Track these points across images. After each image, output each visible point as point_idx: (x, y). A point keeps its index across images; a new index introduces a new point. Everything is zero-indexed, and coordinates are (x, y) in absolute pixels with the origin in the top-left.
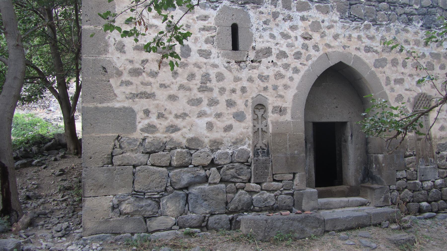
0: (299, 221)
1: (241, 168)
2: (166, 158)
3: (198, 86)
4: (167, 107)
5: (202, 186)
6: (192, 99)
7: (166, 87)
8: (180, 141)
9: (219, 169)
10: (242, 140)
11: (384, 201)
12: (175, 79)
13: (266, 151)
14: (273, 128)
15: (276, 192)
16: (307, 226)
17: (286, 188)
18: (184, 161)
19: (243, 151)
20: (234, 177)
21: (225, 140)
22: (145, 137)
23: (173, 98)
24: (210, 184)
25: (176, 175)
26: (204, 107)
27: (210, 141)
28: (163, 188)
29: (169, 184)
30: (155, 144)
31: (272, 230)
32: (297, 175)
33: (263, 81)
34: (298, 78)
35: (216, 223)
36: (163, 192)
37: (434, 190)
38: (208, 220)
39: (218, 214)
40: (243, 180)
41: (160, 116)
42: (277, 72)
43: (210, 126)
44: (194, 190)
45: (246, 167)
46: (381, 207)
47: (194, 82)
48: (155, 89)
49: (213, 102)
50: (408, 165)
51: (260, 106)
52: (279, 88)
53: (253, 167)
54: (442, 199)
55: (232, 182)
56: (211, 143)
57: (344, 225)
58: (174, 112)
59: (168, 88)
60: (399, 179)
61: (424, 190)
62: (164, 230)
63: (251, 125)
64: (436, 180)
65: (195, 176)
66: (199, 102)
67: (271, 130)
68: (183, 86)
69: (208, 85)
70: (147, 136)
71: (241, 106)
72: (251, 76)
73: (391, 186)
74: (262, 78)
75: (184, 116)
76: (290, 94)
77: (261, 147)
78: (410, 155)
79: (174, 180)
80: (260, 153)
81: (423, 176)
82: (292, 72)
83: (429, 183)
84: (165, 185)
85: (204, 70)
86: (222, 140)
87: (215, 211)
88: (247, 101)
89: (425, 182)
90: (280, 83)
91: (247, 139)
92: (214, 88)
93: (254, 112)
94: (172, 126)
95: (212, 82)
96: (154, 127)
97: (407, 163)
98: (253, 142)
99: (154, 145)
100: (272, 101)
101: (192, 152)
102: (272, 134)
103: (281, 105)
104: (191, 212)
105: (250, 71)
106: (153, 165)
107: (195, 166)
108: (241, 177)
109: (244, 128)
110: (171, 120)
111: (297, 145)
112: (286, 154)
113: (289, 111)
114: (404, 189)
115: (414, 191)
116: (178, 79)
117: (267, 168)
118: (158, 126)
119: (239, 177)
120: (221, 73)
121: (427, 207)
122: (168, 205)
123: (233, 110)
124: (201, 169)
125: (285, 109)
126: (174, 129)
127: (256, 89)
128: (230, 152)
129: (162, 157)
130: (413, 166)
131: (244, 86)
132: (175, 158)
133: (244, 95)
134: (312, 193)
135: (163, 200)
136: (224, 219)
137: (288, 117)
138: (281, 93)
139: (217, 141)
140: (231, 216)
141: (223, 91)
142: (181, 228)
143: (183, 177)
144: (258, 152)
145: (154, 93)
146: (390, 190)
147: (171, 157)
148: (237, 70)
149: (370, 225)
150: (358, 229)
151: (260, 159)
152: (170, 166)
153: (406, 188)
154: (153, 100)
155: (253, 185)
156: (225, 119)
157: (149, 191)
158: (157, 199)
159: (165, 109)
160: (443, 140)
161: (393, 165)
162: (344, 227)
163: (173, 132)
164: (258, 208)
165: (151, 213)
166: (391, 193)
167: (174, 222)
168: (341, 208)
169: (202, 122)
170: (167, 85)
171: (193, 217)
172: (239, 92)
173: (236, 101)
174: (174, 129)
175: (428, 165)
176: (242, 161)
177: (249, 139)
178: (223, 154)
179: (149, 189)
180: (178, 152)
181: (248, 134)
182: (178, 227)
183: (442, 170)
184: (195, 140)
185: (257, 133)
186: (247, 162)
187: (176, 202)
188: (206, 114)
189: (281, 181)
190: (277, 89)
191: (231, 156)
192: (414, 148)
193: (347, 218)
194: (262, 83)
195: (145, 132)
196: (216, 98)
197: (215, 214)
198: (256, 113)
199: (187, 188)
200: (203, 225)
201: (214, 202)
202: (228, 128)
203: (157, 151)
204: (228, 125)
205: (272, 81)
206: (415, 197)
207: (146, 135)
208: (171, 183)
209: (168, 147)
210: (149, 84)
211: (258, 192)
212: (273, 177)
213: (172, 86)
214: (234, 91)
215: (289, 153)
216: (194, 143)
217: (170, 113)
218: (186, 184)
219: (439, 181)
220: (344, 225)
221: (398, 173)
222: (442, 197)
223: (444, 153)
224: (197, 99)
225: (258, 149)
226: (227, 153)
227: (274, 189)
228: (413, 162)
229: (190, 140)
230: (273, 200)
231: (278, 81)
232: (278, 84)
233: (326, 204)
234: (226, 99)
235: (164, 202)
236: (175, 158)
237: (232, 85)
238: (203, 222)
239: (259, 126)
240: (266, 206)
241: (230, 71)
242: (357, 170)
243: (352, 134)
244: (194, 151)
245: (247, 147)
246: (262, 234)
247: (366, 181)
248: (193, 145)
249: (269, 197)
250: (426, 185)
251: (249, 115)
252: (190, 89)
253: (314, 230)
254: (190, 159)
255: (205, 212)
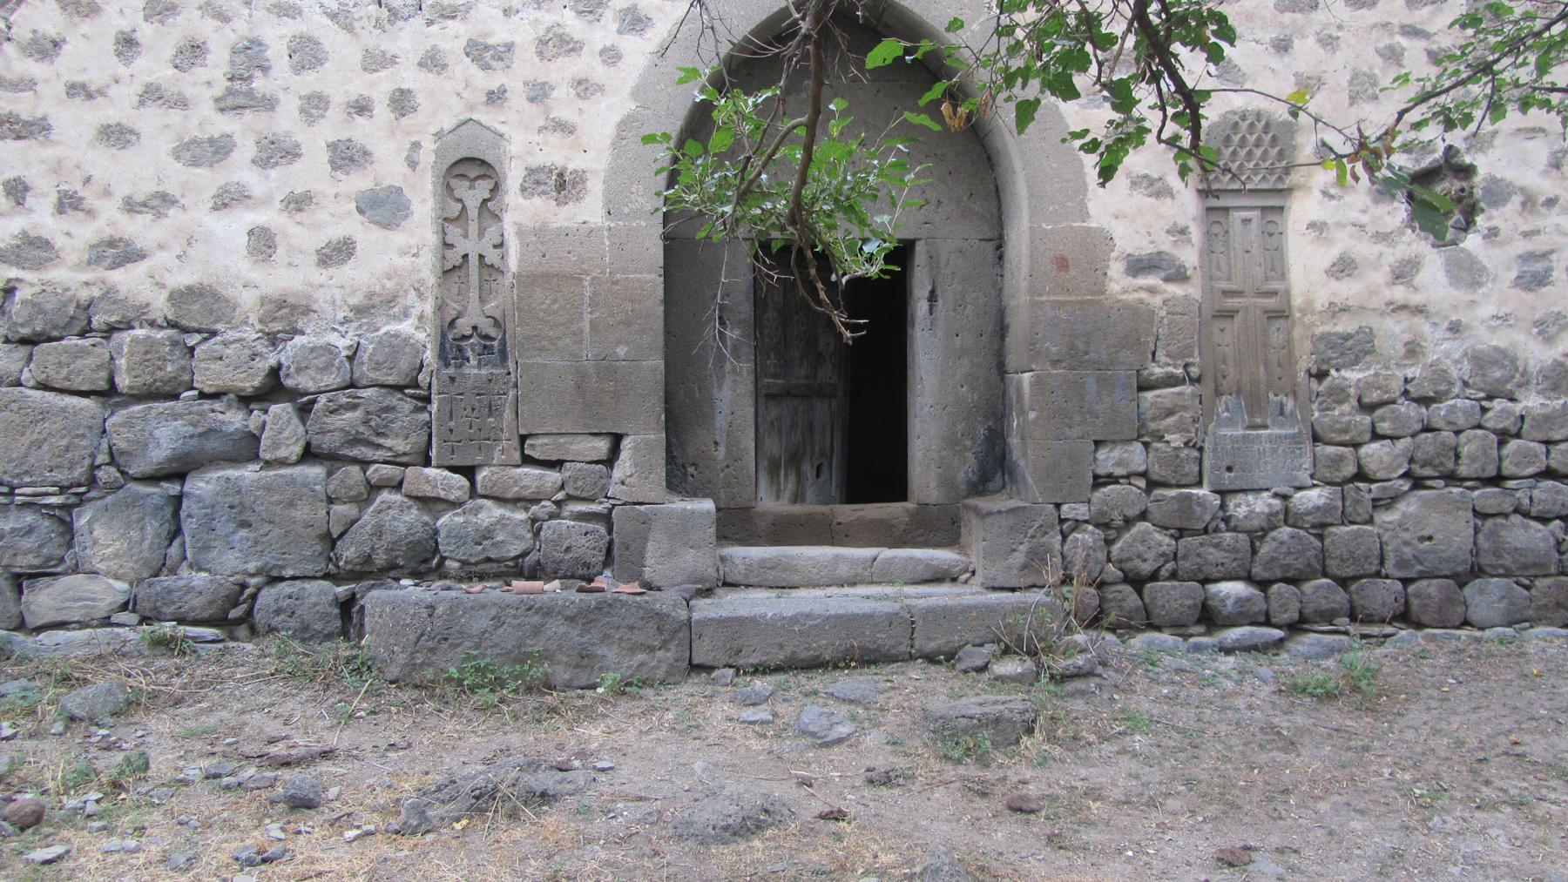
0: (571, 619)
1: (388, 409)
2: (90, 361)
3: (219, 90)
4: (93, 172)
5: (233, 473)
6: (194, 141)
7: (90, 96)
8: (143, 300)
9: (304, 411)
10: (391, 300)
11: (1024, 567)
12: (128, 62)
13: (496, 343)
14: (523, 255)
15: (534, 508)
16: (605, 638)
17: (578, 493)
18: (159, 374)
19: (396, 342)
20: (357, 441)
21: (321, 299)
22: (9, 280)
23: (116, 135)
24: (268, 464)
25: (129, 424)
26: (240, 170)
27: (263, 301)
28: (79, 472)
29: (102, 458)
30: (49, 307)
31: (445, 645)
32: (626, 443)
33: (486, 67)
34: (638, 50)
35: (278, 612)
36: (80, 485)
37: (1285, 532)
38: (254, 597)
39: (293, 578)
40: (398, 455)
41: (68, 203)
42: (549, 30)
43: (263, 243)
44: (202, 485)
45: (407, 406)
46: (1013, 590)
47: (200, 73)
48: (47, 102)
49: (276, 152)
50: (1153, 419)
51: (470, 169)
52: (555, 94)
53: (434, 407)
54: (1325, 575)
55: (355, 461)
56: (267, 307)
57: (781, 646)
58: (122, 190)
59: (100, 99)
60: (1112, 479)
61: (1235, 529)
62: (83, 625)
63: (431, 238)
64: (1300, 488)
65: (200, 430)
66: (220, 149)
67: (513, 264)
68: (158, 89)
69: (259, 84)
70: (18, 280)
71: (389, 167)
72: (434, 47)
73: (1065, 508)
74: (481, 53)
75: (160, 203)
76: (601, 121)
77: (475, 328)
78: (1170, 381)
79: (122, 445)
80: (469, 354)
81: (1229, 469)
82: (615, 26)
84: (87, 462)
85: (240, 28)
86: (309, 297)
87: (283, 567)
88: (416, 145)
89: (1240, 498)
90: (562, 71)
91: (412, 293)
92: (281, 95)
93: (449, 188)
94: (112, 243)
95: (272, 72)
96: (43, 244)
97: (1149, 415)
98: (440, 308)
99: (42, 311)
100: (522, 146)
101: (192, 340)
102: (517, 276)
103: (560, 164)
104: (191, 566)
105: (435, 28)
106: (44, 386)
107: (203, 395)
108: (388, 442)
109: (402, 255)
110: (110, 219)
111: (628, 324)
112: (575, 356)
113: (596, 188)
114: (1129, 522)
115: (1181, 533)
116: (140, 63)
117: (492, 410)
118: (59, 241)
119: (381, 441)
120: (310, 39)
121: (1240, 601)
122: (95, 533)
123: (359, 182)
124: (229, 407)
125: (580, 178)
126: (121, 252)
127: (455, 100)
128: (343, 343)
129: (79, 358)
130: (1179, 428)
131: (405, 86)
132: (123, 361)
133: (405, 121)
134: (688, 516)
135: (79, 516)
136: (313, 599)
137: (589, 210)
138: (565, 113)
139: (291, 300)
140: (342, 590)
141: (317, 107)
142: (145, 620)
143: (157, 433)
144: (460, 349)
145: (44, 119)
146: (1062, 521)
147: (112, 358)
148: (378, 24)
149: (912, 658)
150: (848, 667)
151: (464, 376)
152: (108, 393)
153: (1143, 516)
154: (42, 144)
155: (436, 479)
156: (322, 216)
157: (27, 479)
158: (57, 512)
159: (88, 180)
160: (1345, 317)
161: (1077, 419)
162: (779, 657)
163: (115, 265)
164: (456, 565)
165: (36, 562)
166: (1064, 537)
167: (122, 599)
168: (840, 580)
169: (234, 227)
170: (93, 88)
171: (197, 583)
172: (382, 111)
173: (369, 148)
174: (121, 252)
175: (1265, 427)
176: (391, 380)
177: (420, 295)
178: (313, 350)
179: (26, 473)
180: (135, 340)
181: (415, 277)
182: (134, 618)
183: (1330, 449)
184: (201, 295)
185: (462, 273)
186: (417, 386)
187: (128, 526)
188: (248, 197)
189: (556, 464)
190: (546, 95)
191: (351, 359)
192: (1190, 347)
193: (794, 619)
194: (482, 73)
195: (11, 263)
196: (288, 134)
197: (282, 579)
198: (457, 194)
199: (179, 475)
200: (233, 615)
201: (277, 531)
202: (338, 253)
203: (55, 334)
204: (335, 239)
205: (526, 66)
206: (1185, 557)
207: (14, 273)
208: (111, 454)
209: (98, 321)
210: (29, 84)
211: (460, 504)
212: (522, 449)
213: (113, 91)
214: (362, 108)
215: (588, 352)
216: (196, 307)
217: (107, 193)
218: (170, 460)
219: (1313, 497)
220: (781, 646)
221: (1102, 454)
222: (1324, 566)
223: (1345, 373)
224: (211, 141)
225: (465, 338)
226: (329, 349)
227: (526, 493)
228: (1185, 408)
229: (181, 294)
230: (520, 538)
231: (552, 66)
232: (553, 78)
233: (773, 565)
234: (330, 140)
235: (83, 521)
236: (123, 361)
237: (359, 84)
238: (236, 604)
239: (469, 245)
240: (489, 560)
241: (349, 28)
242: (951, 441)
243: (932, 292)
244: (197, 338)
245: (414, 328)
246: (402, 658)
247: (990, 486)
248: (195, 316)
249: (501, 522)
250: (1241, 512)
251: (424, 201)
252: (182, 103)
253: (641, 657)
254: (183, 369)
255: (241, 567)
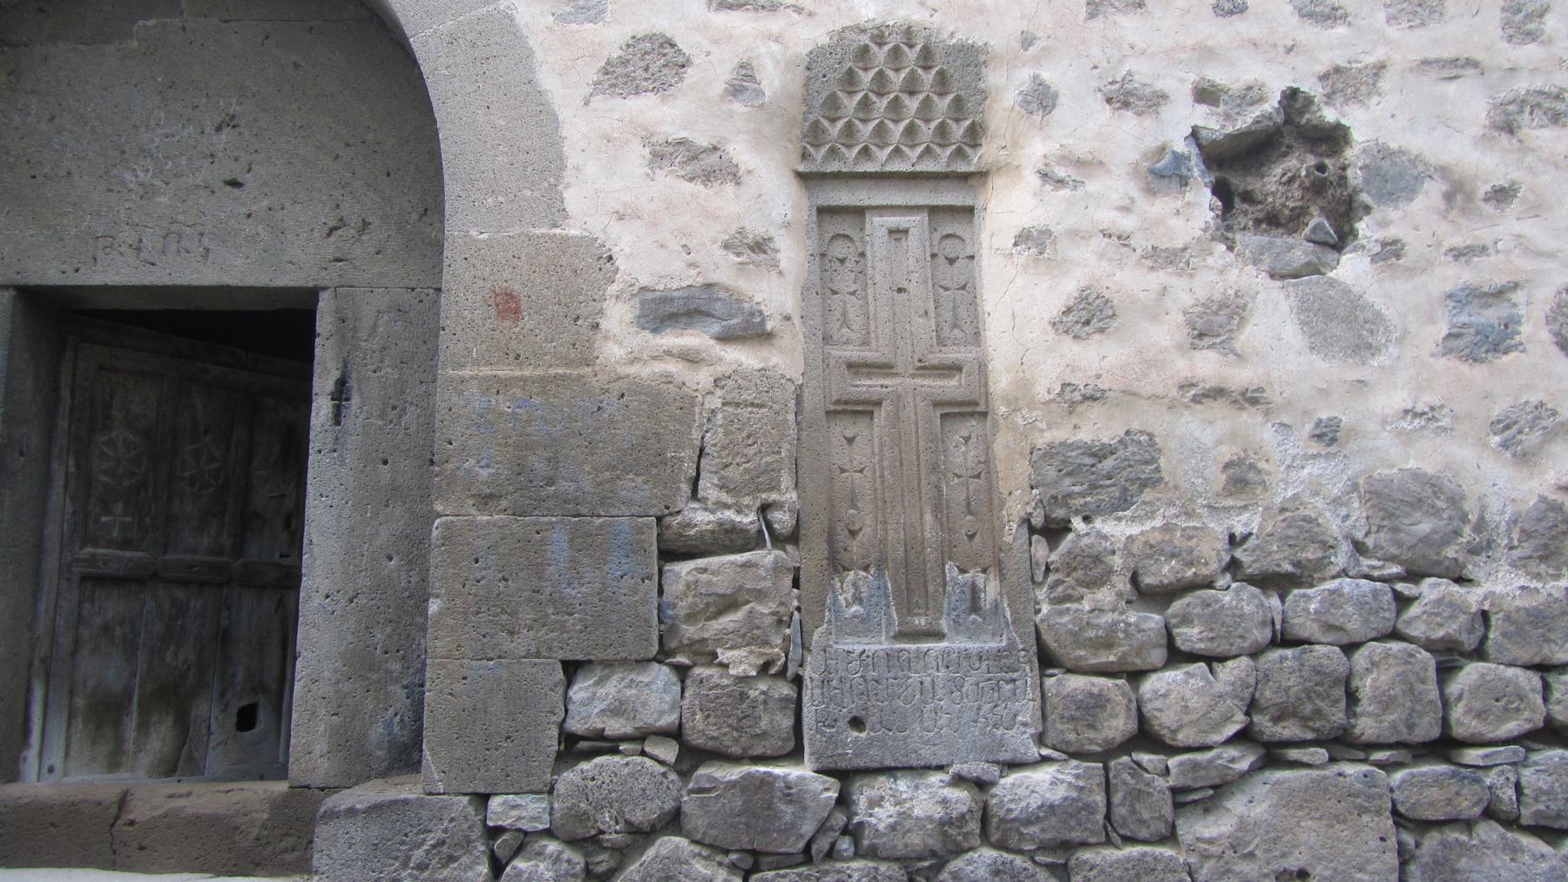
50: (691, 617)
60: (605, 744)
61: (873, 853)
64: (1013, 765)
73: (495, 803)
78: (730, 540)
81: (857, 723)
83: (926, 800)
89: (882, 784)
114: (642, 835)
130: (749, 636)
146: (494, 832)
153: (673, 821)
160: (1095, 412)
161: (527, 615)
175: (939, 636)
183: (1076, 683)
192: (770, 469)
219: (1042, 785)
228: (760, 595)
250: (883, 816)
